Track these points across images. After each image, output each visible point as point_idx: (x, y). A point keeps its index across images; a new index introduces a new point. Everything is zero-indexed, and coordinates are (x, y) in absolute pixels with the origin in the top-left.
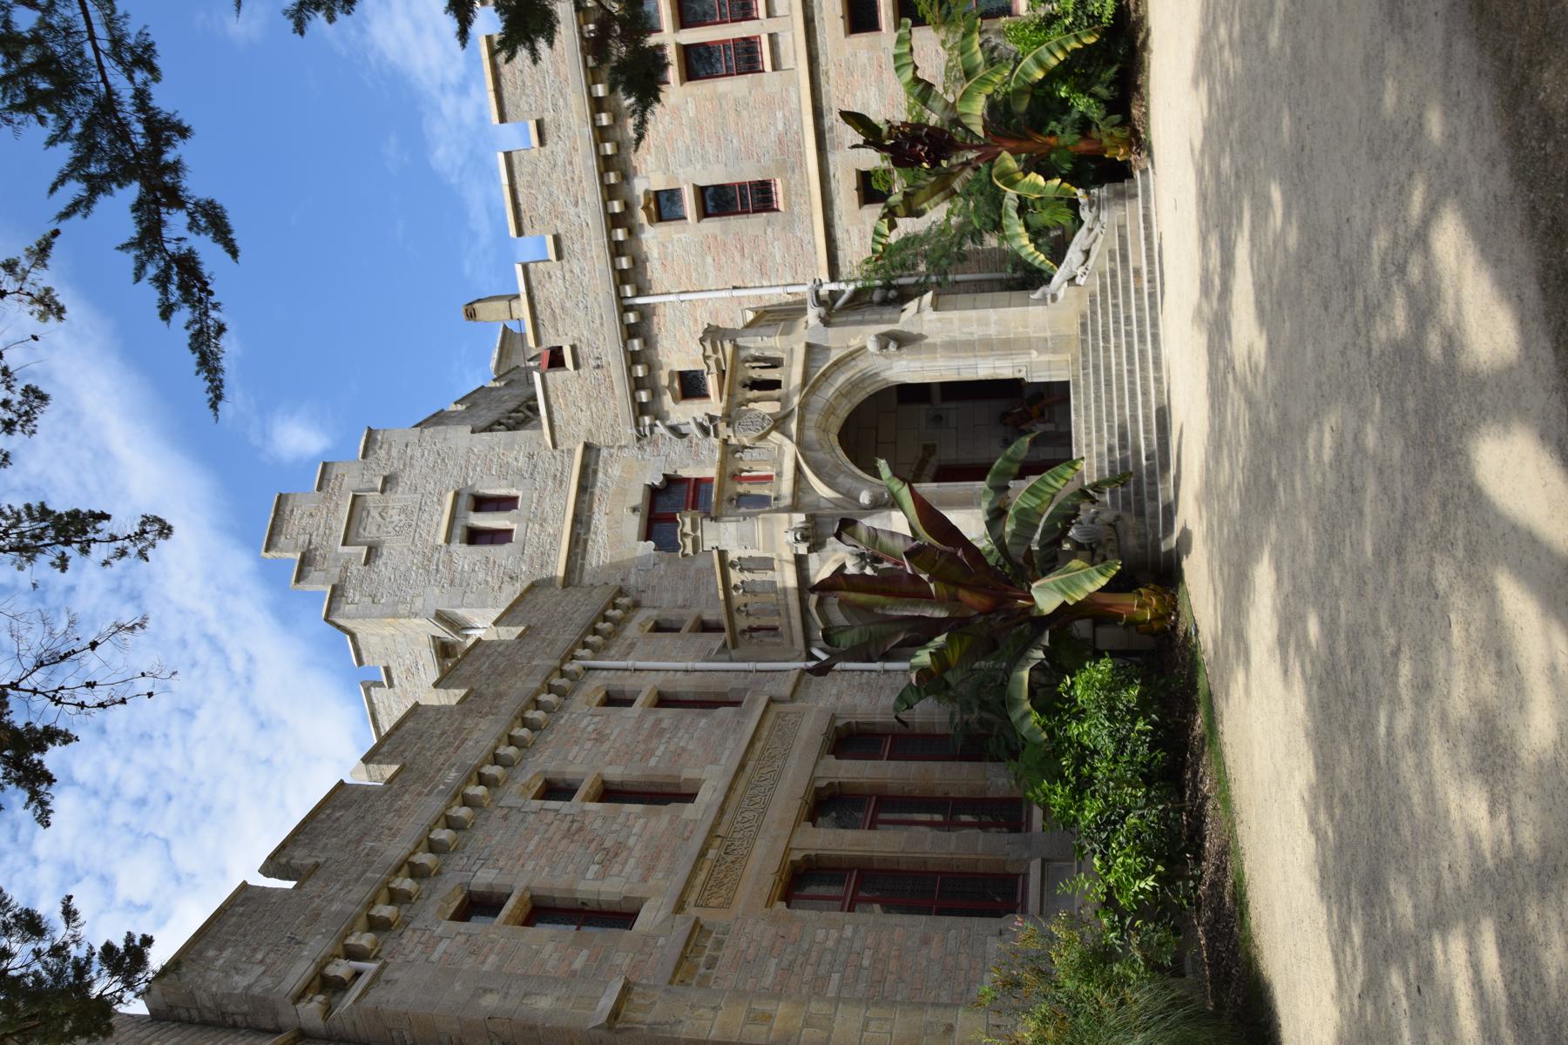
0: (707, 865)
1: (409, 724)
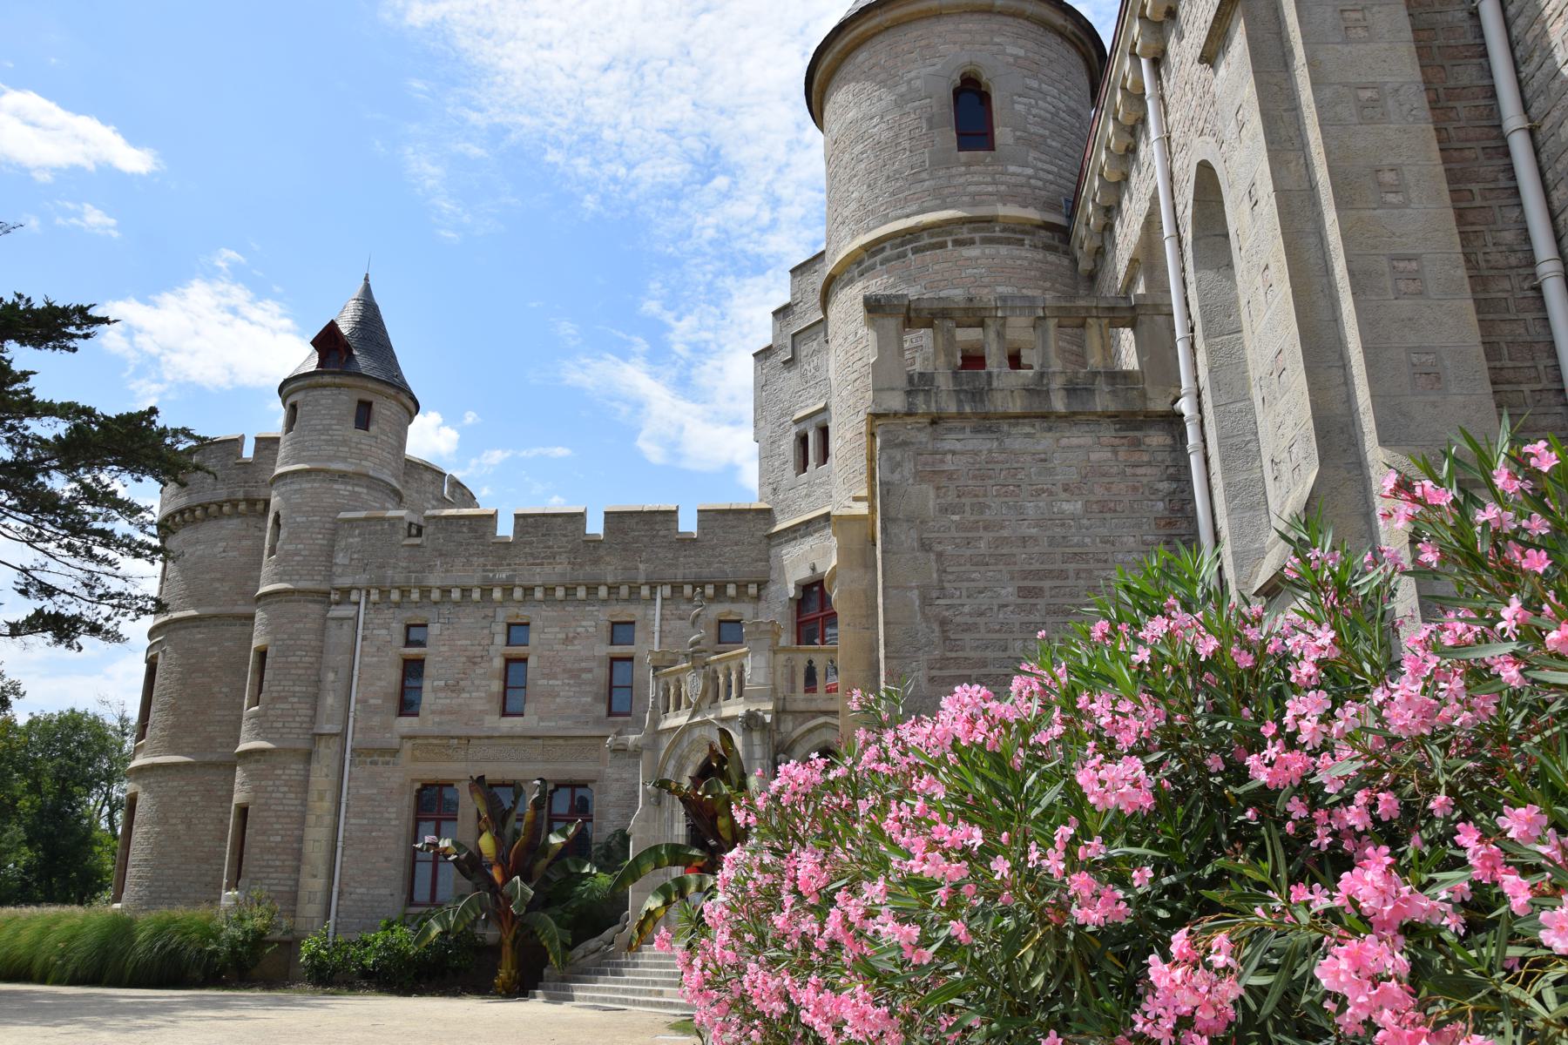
0: (444, 741)
1: (560, 519)
